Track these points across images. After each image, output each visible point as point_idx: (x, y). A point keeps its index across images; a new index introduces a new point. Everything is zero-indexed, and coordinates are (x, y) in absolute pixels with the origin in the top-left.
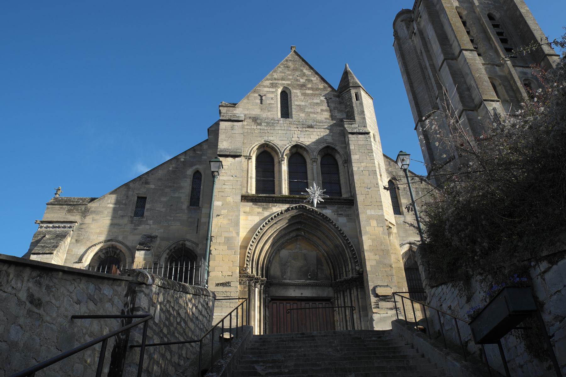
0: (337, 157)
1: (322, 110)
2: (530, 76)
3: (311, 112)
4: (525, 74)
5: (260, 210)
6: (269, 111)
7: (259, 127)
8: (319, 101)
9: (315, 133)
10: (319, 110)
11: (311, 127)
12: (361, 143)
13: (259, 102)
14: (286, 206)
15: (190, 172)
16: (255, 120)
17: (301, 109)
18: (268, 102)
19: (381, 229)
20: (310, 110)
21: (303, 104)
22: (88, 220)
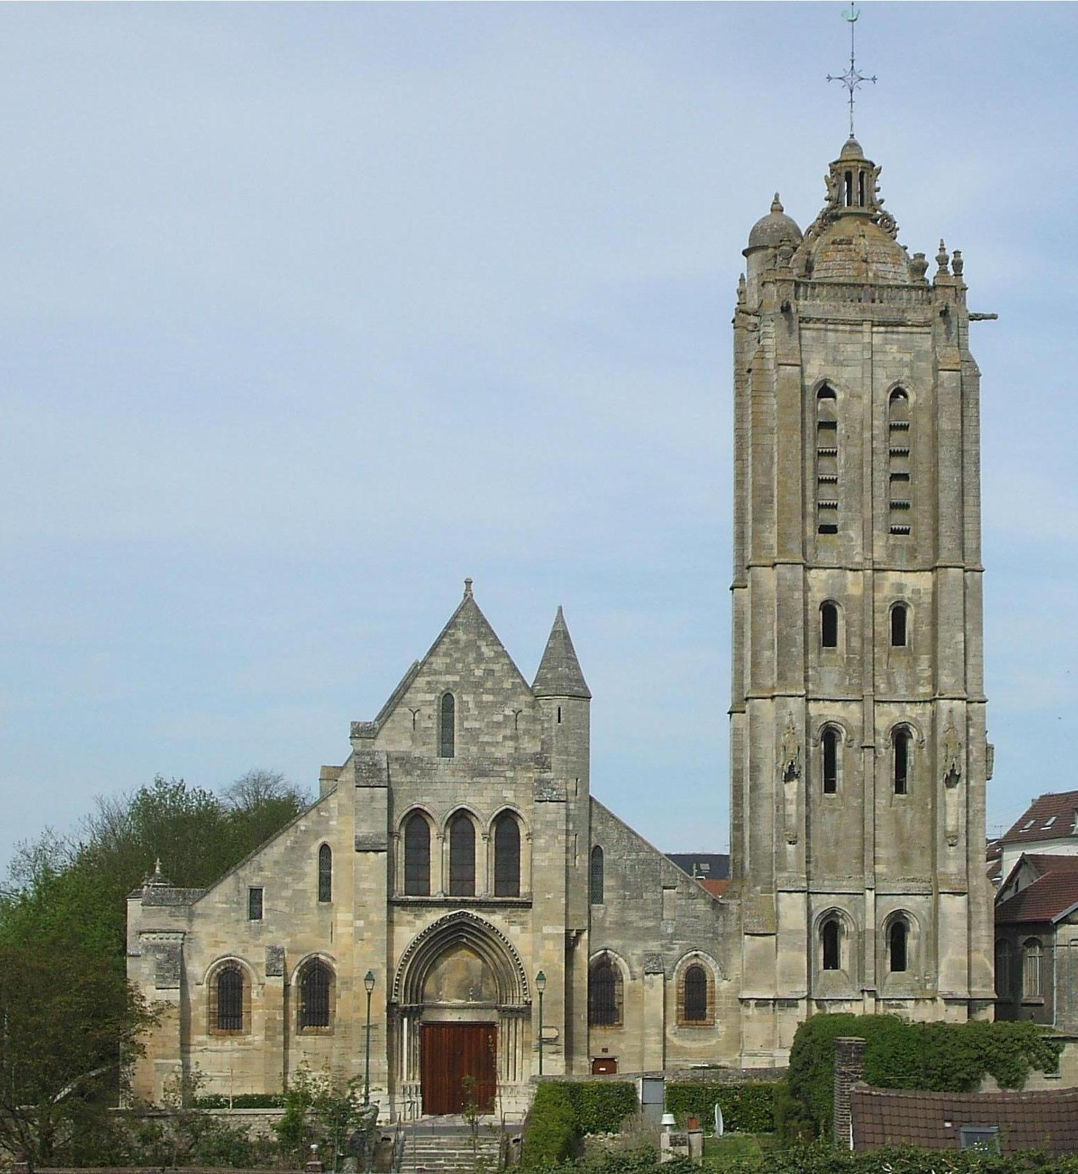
0: (520, 823)
1: (505, 737)
2: (907, 594)
3: (488, 743)
4: (900, 587)
5: (411, 918)
6: (424, 744)
7: (409, 778)
8: (501, 718)
9: (490, 786)
10: (500, 739)
11: (484, 774)
12: (549, 817)
13: (410, 725)
14: (443, 913)
15: (315, 849)
16: (405, 761)
17: (473, 735)
18: (423, 725)
19: (558, 954)
20: (486, 739)
21: (476, 725)
22: (199, 927)
